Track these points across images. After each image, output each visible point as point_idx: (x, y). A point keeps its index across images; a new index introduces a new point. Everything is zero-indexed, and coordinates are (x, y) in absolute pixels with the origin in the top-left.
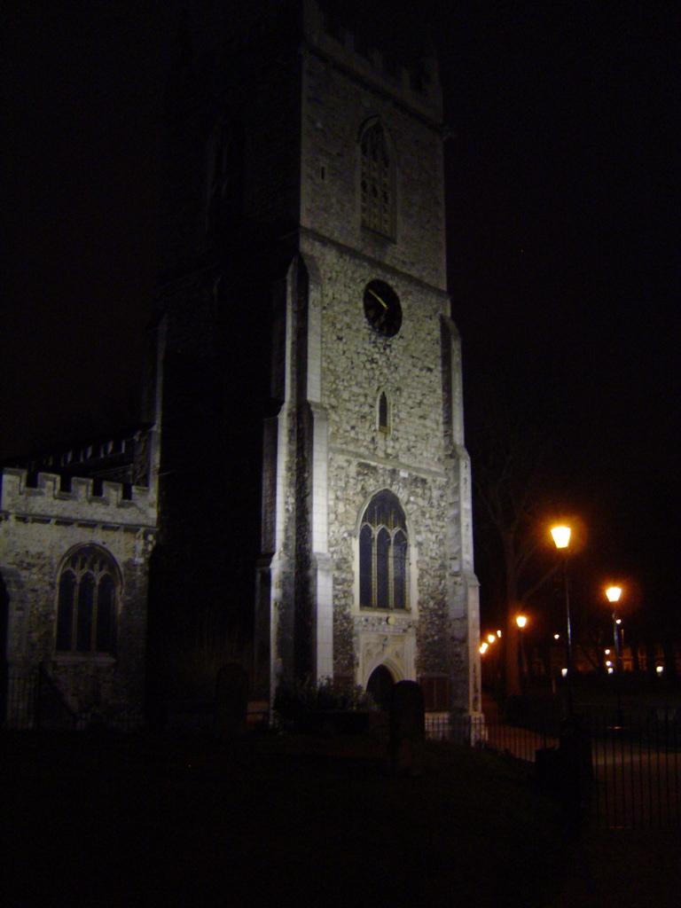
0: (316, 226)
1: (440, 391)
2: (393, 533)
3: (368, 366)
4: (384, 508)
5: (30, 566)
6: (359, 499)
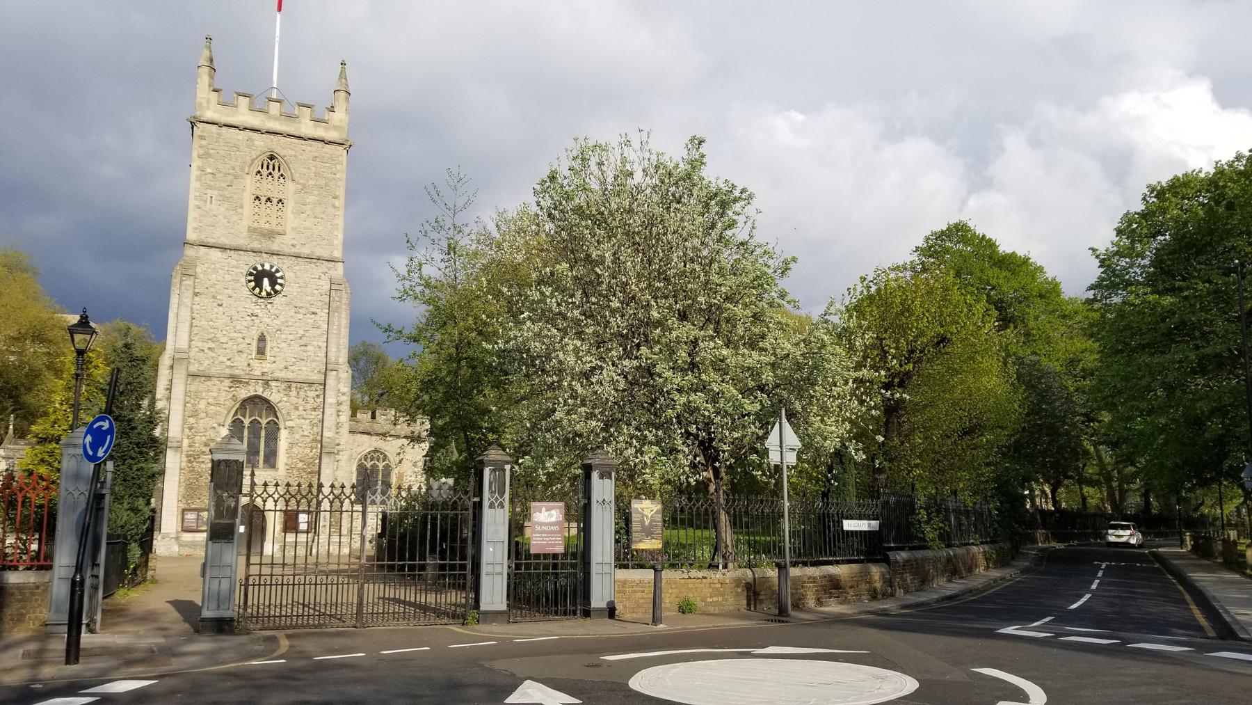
2: (264, 422)
6: (230, 403)
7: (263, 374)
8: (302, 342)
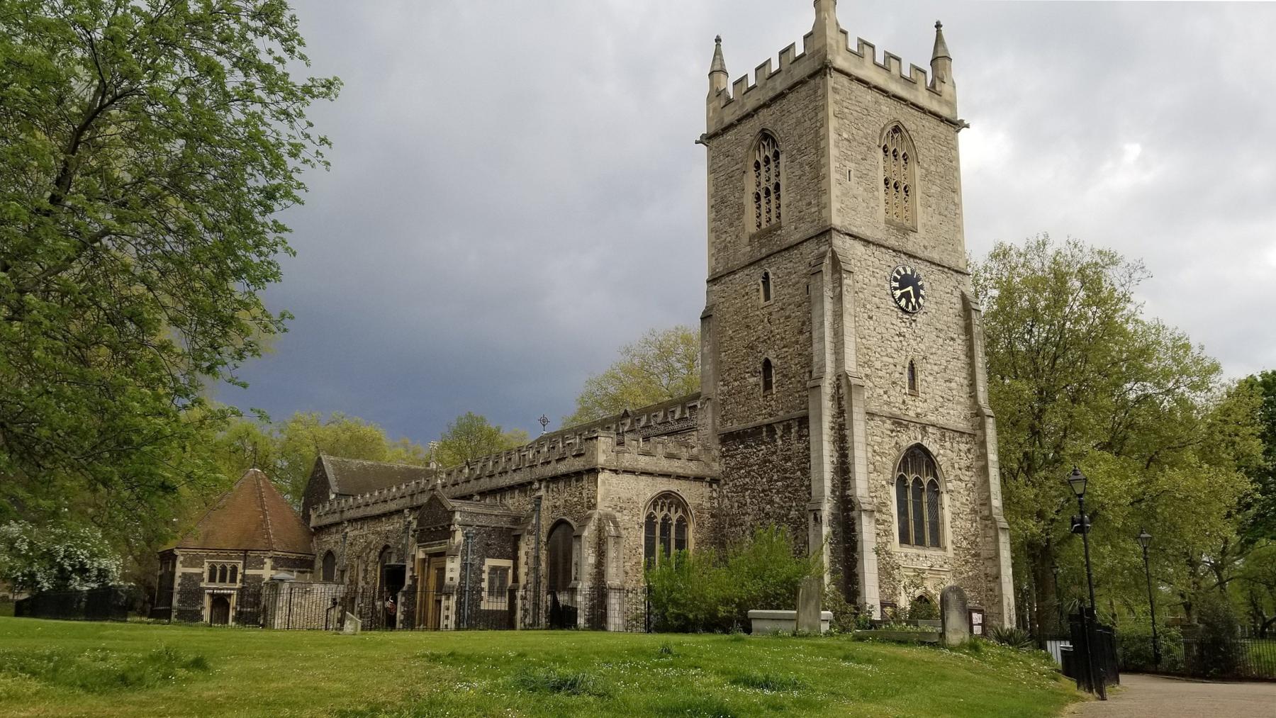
0: (846, 223)
1: (963, 357)
2: (926, 480)
3: (896, 338)
4: (917, 459)
5: (621, 510)
6: (894, 452)
7: (918, 415)
8: (946, 376)
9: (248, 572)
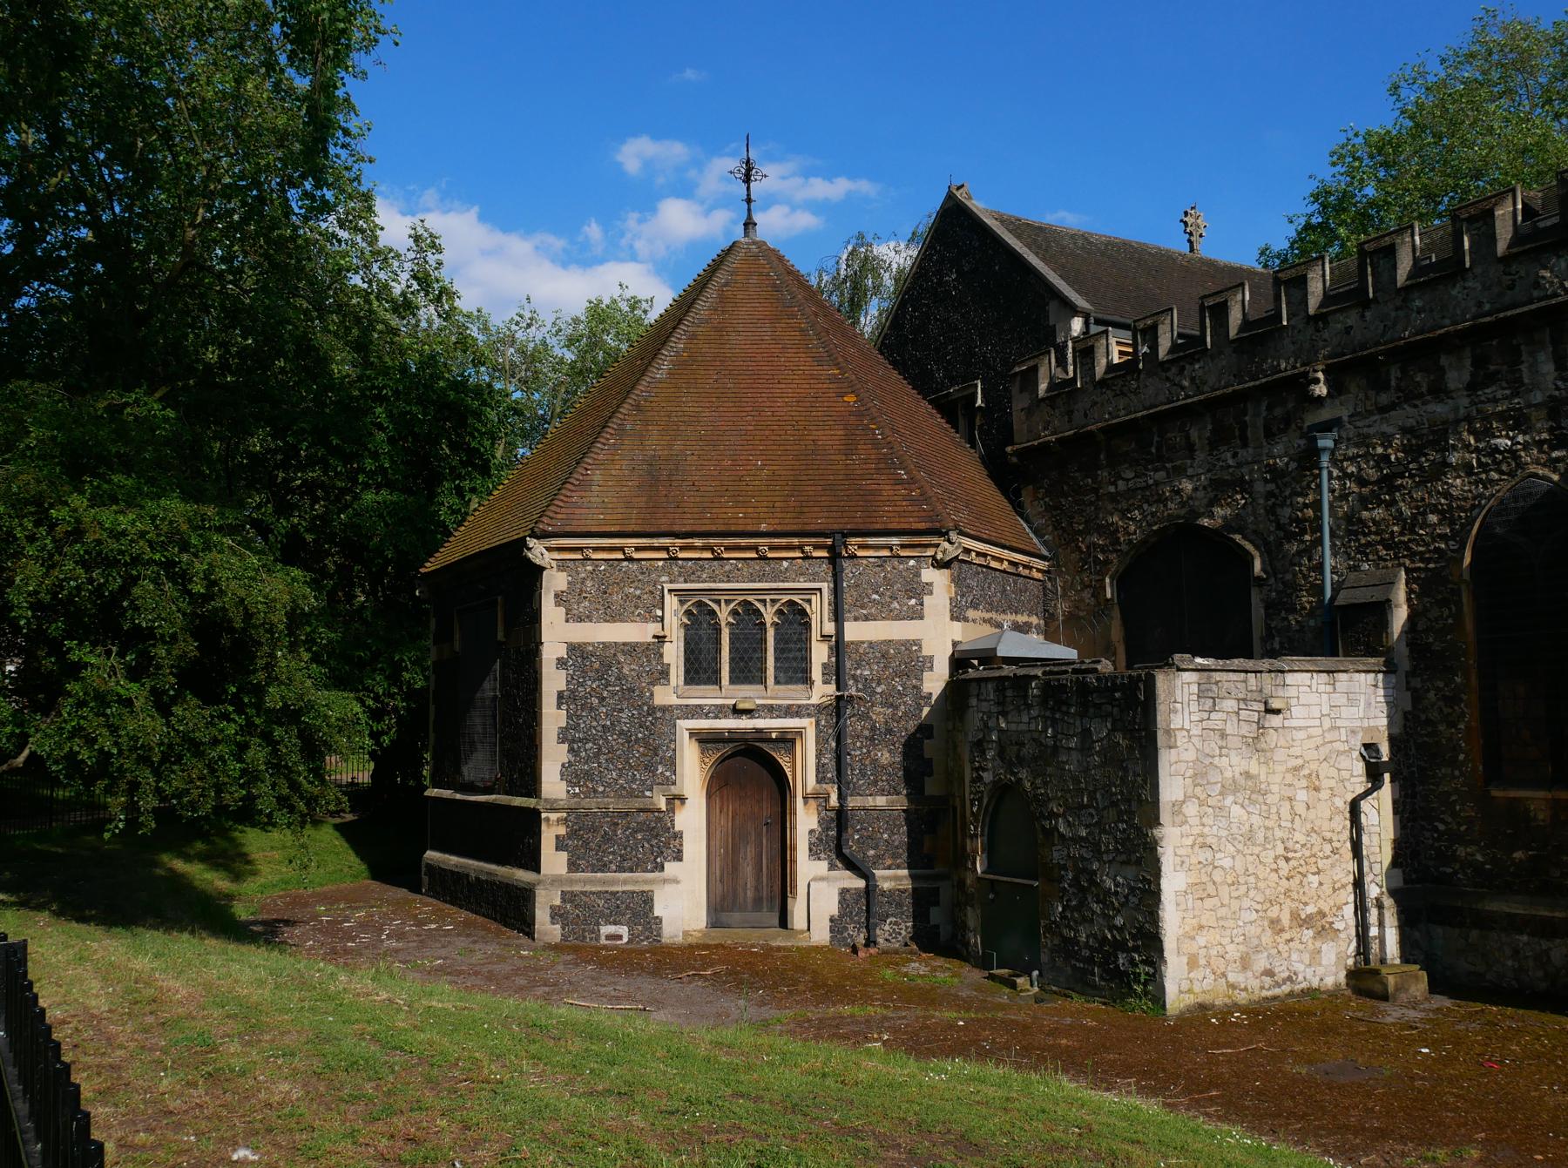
9: (855, 631)
